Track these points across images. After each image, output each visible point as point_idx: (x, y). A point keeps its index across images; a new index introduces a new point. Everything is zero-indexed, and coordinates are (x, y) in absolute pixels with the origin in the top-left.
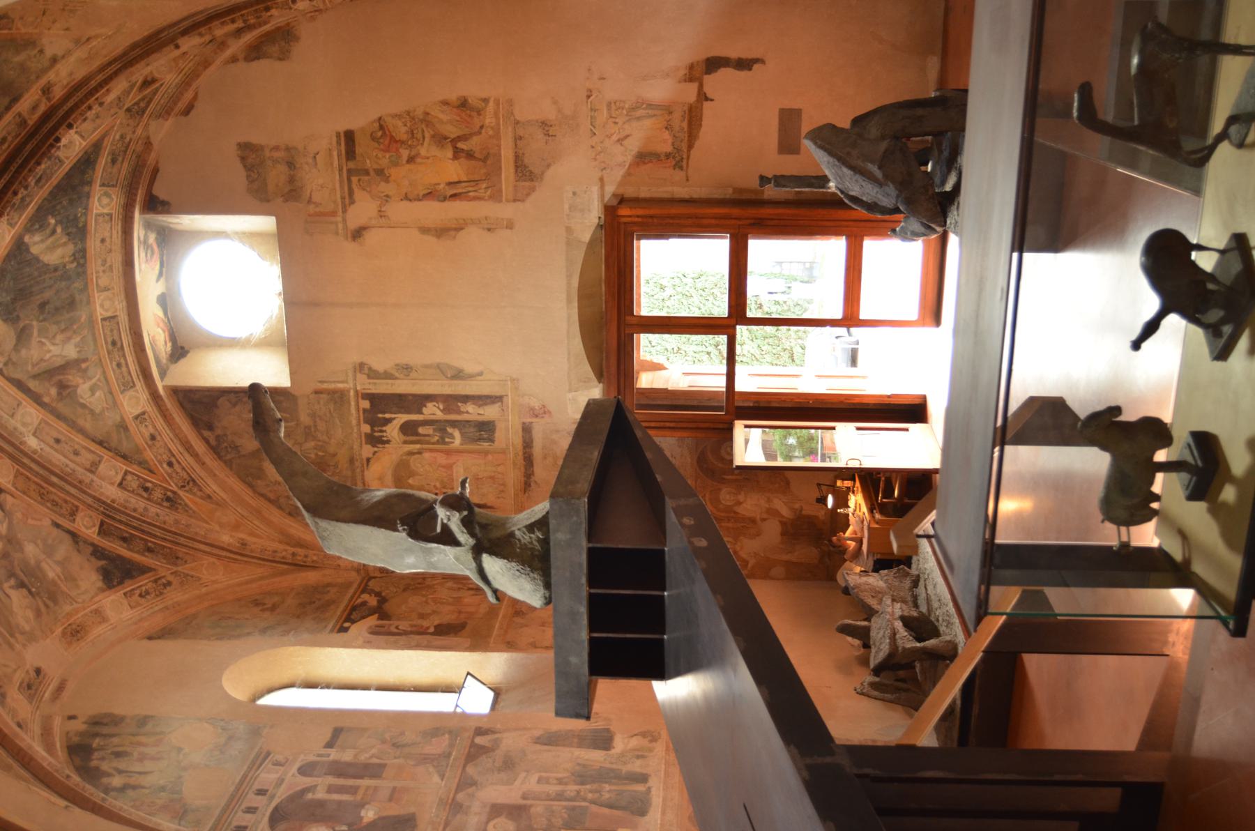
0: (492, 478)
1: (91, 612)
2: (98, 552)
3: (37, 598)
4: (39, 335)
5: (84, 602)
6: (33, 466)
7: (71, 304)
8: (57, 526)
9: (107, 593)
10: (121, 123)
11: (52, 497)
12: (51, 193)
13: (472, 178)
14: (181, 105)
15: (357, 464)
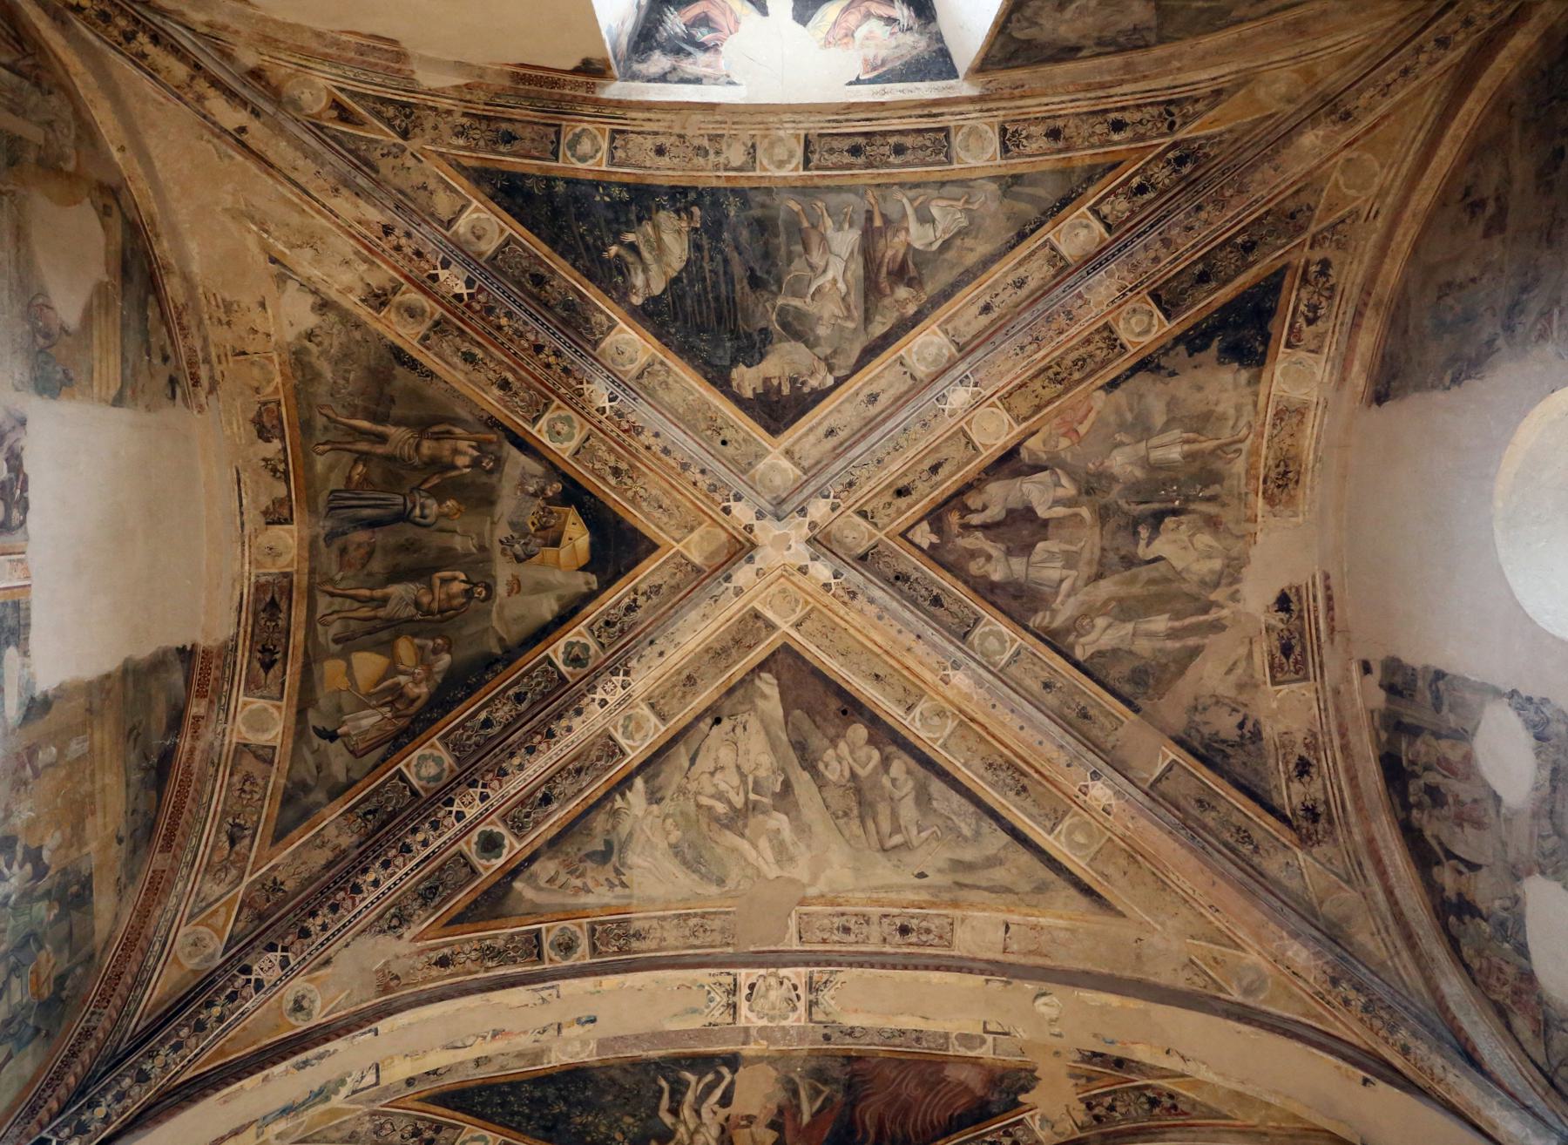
1: (1274, 426)
2: (1194, 341)
3: (1192, 506)
4: (802, 296)
5: (1250, 425)
7: (763, 226)
8: (1113, 385)
9: (1266, 375)
10: (433, 141)
11: (1068, 362)
12: (563, 256)
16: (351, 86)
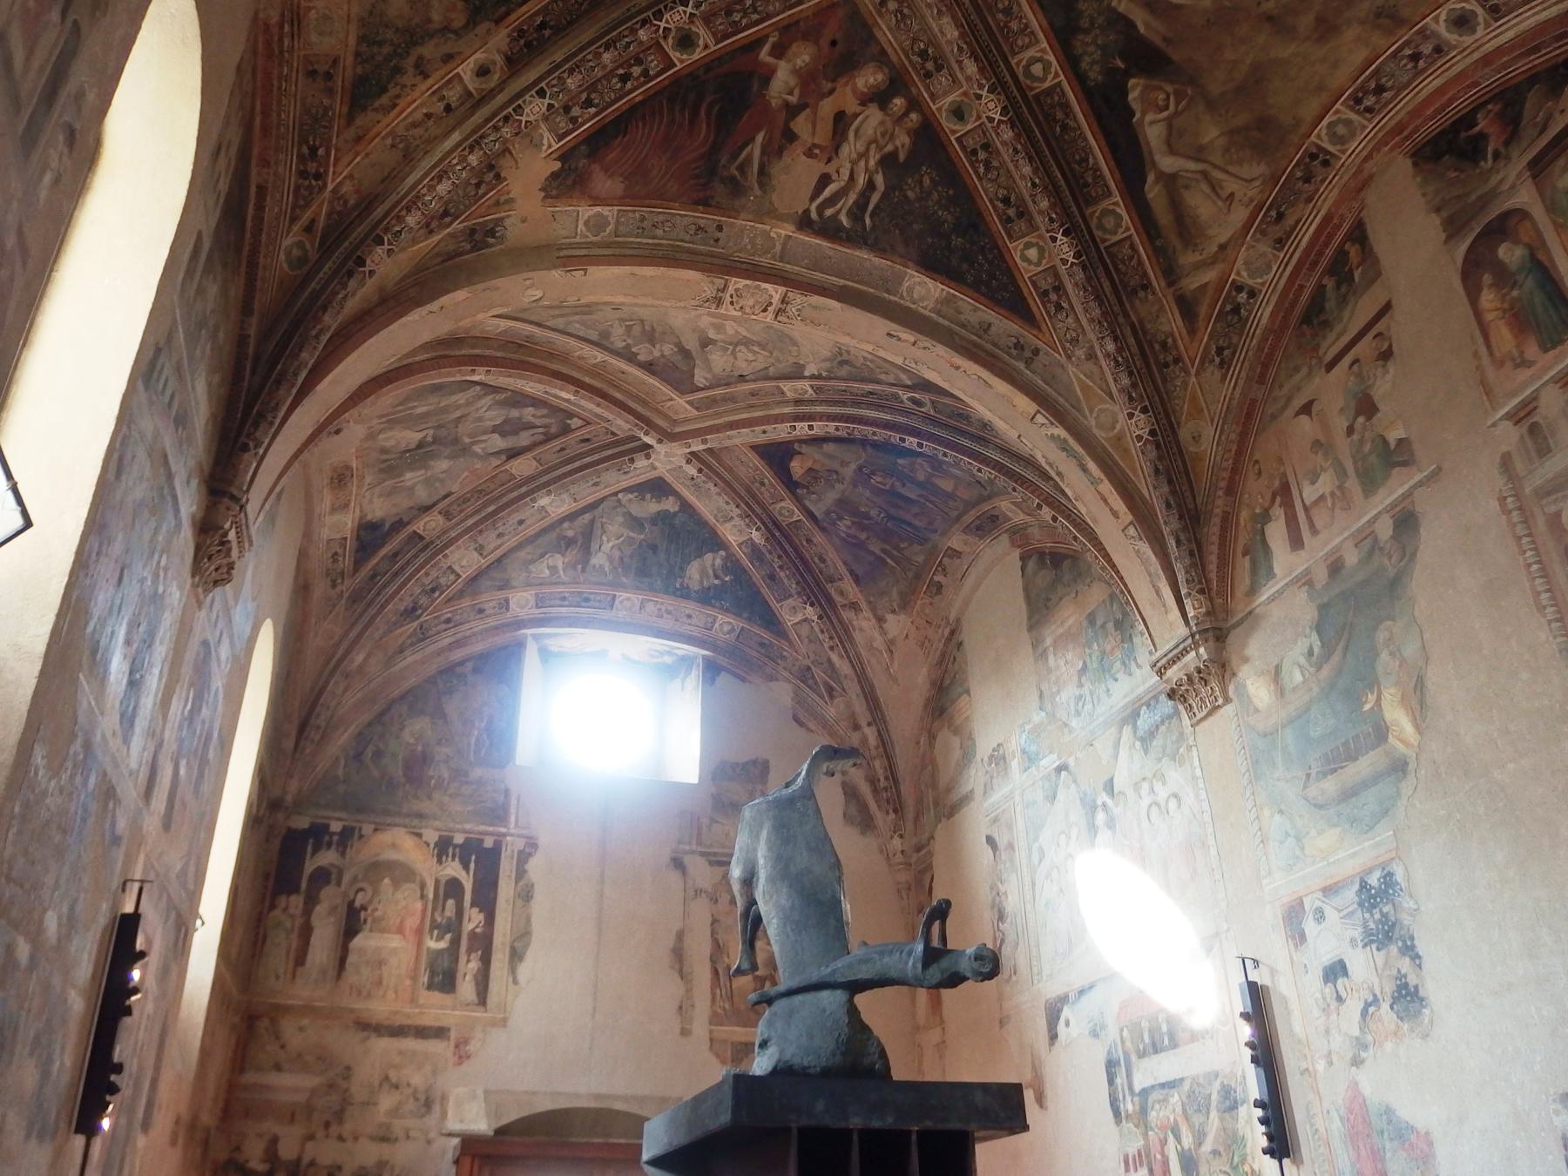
0: (379, 983)
6: (515, 494)
7: (643, 572)
8: (446, 497)
11: (472, 500)
13: (735, 992)
14: (802, 715)
15: (416, 822)
16: (821, 702)
